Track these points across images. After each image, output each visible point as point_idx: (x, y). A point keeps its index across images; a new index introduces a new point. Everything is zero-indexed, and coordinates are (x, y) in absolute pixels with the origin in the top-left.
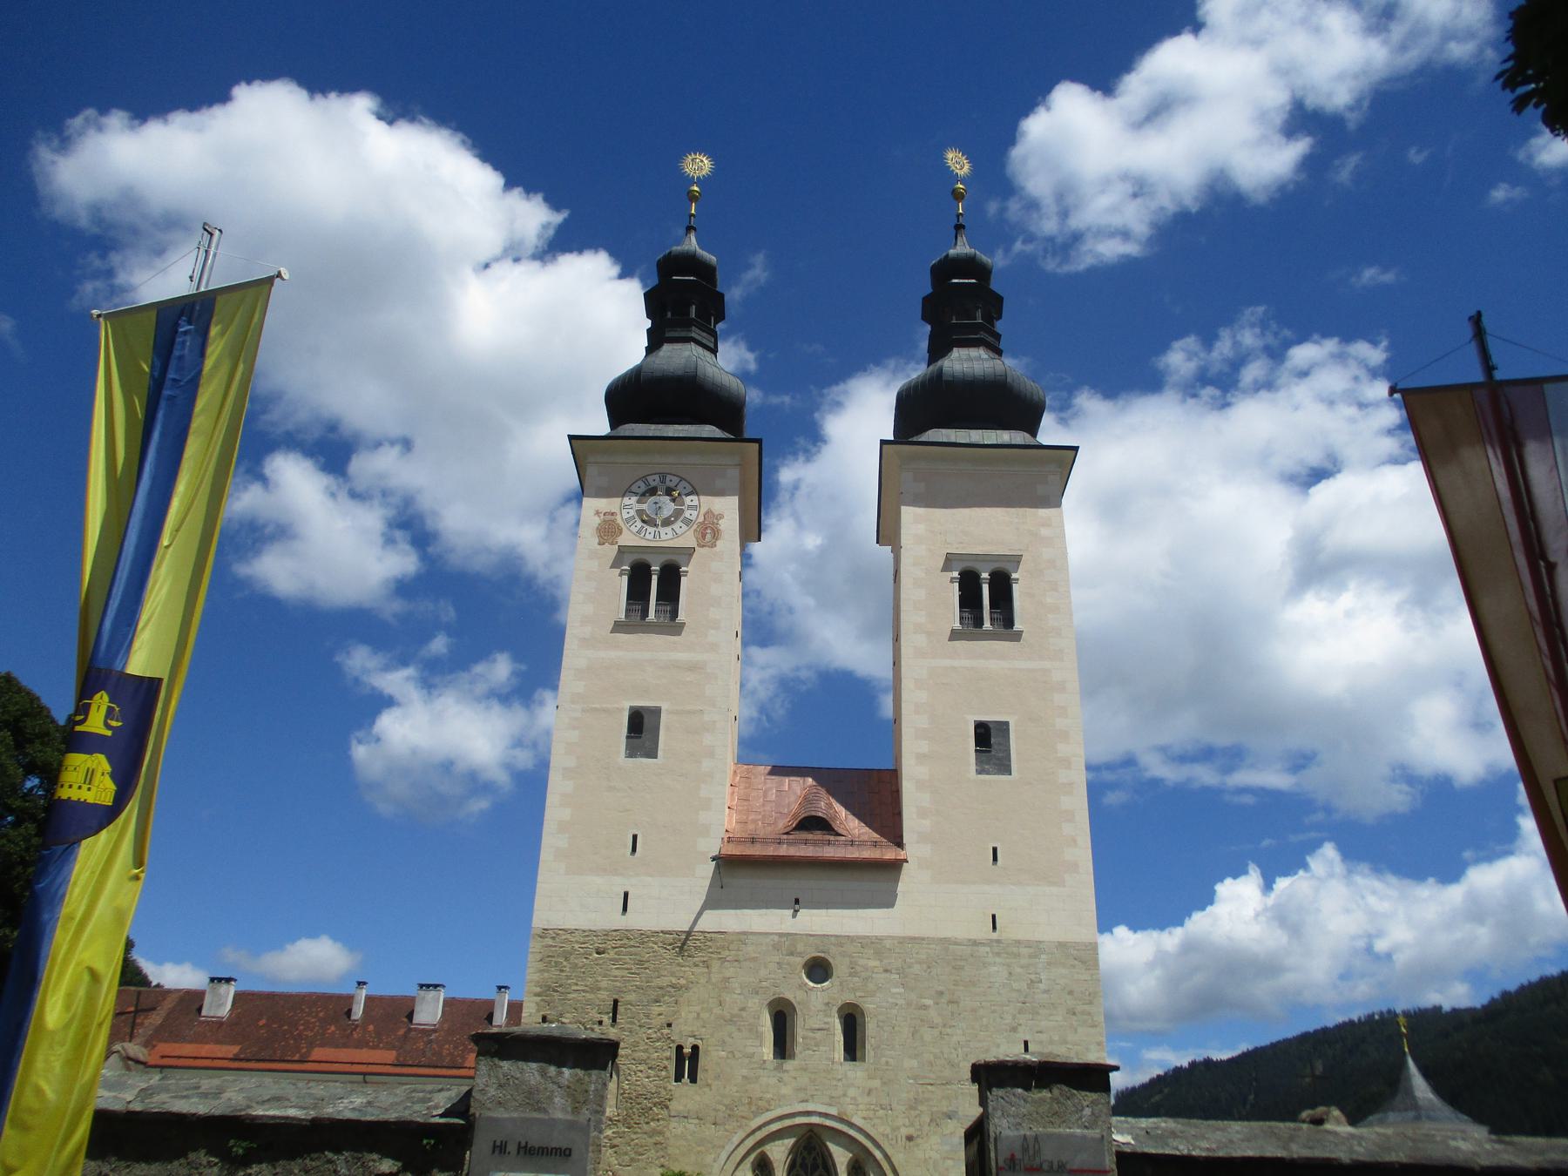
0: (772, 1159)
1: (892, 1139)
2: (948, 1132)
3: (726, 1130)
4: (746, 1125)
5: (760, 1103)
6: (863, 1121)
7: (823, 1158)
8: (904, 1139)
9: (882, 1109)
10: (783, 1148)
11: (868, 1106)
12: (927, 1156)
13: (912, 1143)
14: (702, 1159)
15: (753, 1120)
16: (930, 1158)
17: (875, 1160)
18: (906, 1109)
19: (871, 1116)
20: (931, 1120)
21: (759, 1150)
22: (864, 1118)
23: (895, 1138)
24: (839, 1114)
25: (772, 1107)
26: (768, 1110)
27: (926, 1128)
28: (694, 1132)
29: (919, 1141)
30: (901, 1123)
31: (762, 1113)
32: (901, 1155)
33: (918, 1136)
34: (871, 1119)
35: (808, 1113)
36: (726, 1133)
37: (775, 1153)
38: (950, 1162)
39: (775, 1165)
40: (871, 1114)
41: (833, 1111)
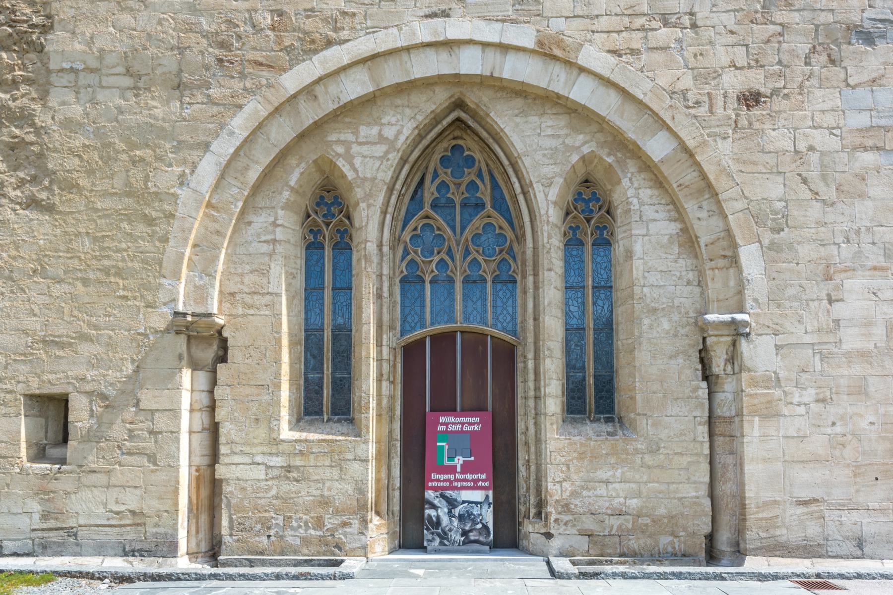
0: (350, 175)
1: (698, 103)
2: (865, 77)
3: (211, 101)
4: (269, 86)
5: (309, 25)
6: (612, 59)
7: (495, 185)
8: (733, 103)
9: (666, 24)
10: (380, 150)
11: (626, 20)
12: (802, 146)
13: (756, 112)
14: (146, 179)
15: (285, 70)
16: (811, 148)
17: (647, 166)
18: (739, 23)
19: (635, 46)
20: (814, 50)
21: (311, 152)
22: (614, 52)
23: (706, 99)
24: (540, 43)
25: (344, 34)
26: (329, 43)
27: (800, 68)
28: (120, 111)
29: (778, 104)
30: (725, 61)
31: (316, 52)
32: (725, 147)
33: (775, 92)
34: (634, 52)
35: (449, 45)
36: (215, 110)
37: (357, 161)
38: (869, 158)
39: (359, 193)
40: (636, 40)
41: (525, 37)
